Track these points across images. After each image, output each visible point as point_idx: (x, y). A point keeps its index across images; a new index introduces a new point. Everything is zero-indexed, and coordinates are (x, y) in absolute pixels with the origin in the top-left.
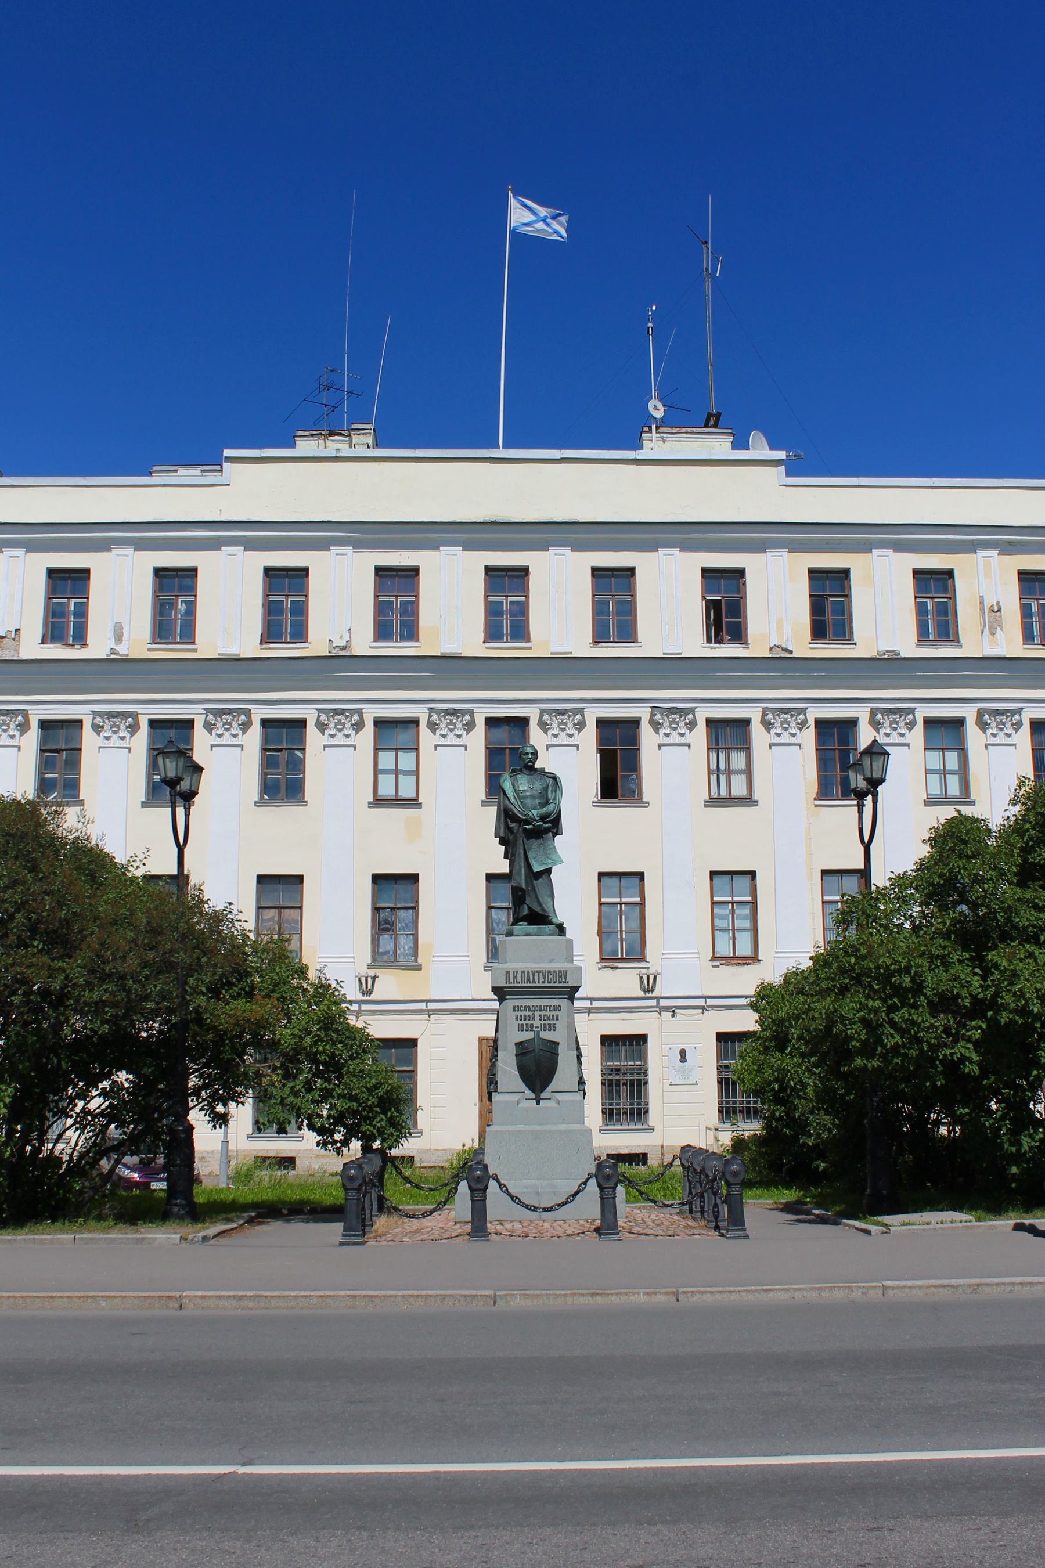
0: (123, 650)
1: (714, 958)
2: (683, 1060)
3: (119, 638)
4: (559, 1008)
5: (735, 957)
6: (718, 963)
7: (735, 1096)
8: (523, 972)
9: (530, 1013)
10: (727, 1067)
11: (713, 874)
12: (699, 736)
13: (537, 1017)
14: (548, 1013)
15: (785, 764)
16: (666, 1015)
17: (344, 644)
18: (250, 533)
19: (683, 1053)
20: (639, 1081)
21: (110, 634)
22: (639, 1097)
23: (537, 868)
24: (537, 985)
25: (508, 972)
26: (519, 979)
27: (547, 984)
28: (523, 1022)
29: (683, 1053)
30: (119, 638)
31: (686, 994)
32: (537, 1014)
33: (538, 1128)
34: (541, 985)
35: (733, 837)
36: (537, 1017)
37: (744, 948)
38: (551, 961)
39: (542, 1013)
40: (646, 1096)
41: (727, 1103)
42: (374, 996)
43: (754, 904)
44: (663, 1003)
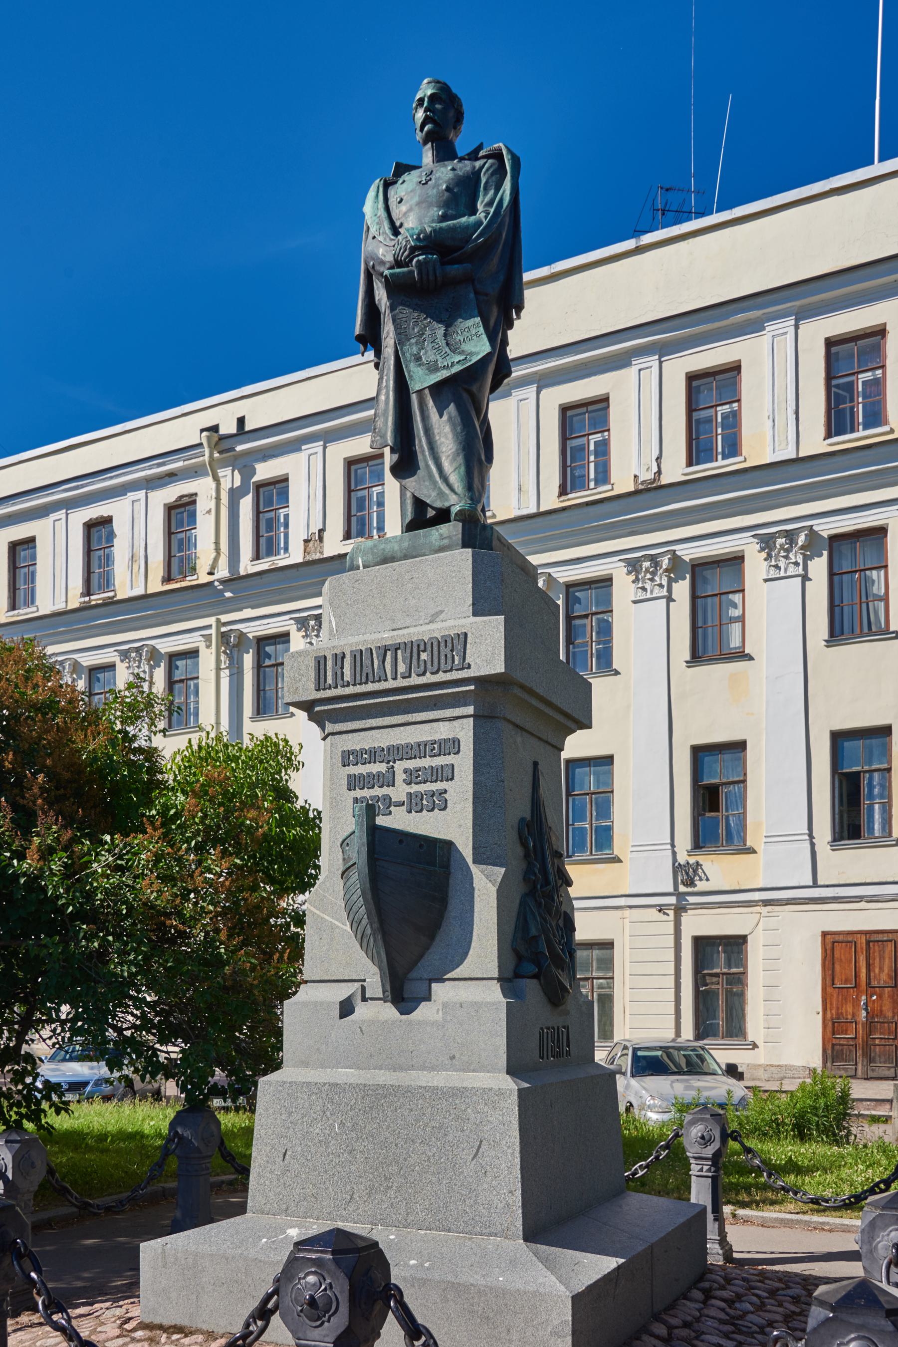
4: (452, 746)
8: (358, 656)
9: (382, 767)
13: (400, 777)
14: (426, 762)
24: (390, 684)
25: (320, 663)
26: (348, 677)
27: (415, 680)
28: (366, 793)
32: (400, 766)
33: (384, 1077)
34: (401, 683)
36: (400, 777)
39: (412, 764)
42: (701, 886)
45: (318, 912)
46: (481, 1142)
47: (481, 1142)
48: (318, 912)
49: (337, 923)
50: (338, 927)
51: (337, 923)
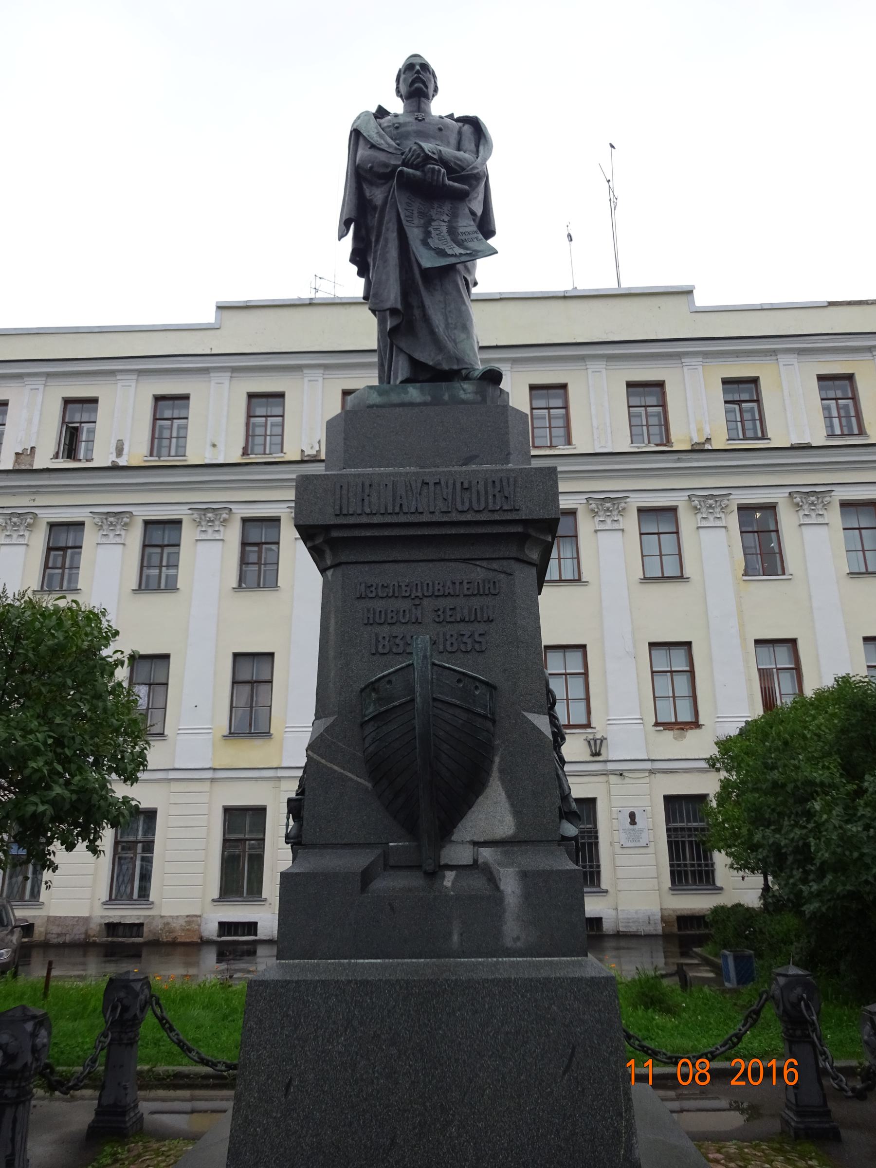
0: (122, 462)
1: (657, 724)
2: (633, 822)
3: (119, 452)
5: (676, 723)
6: (661, 728)
7: (685, 859)
10: (676, 829)
11: (652, 645)
12: (631, 522)
15: (713, 547)
16: (613, 779)
17: (315, 453)
18: (237, 364)
19: (632, 816)
20: (590, 844)
21: (113, 449)
22: (591, 861)
23: (428, 260)
29: (632, 816)
30: (119, 452)
31: (633, 758)
35: (668, 614)
37: (685, 716)
38: (468, 461)
39: (442, 603)
40: (598, 860)
41: (679, 865)
43: (692, 672)
44: (611, 766)
45: (323, 761)
46: (574, 1048)
47: (574, 1048)
48: (323, 761)
49: (349, 775)
50: (351, 779)
51: (349, 775)
